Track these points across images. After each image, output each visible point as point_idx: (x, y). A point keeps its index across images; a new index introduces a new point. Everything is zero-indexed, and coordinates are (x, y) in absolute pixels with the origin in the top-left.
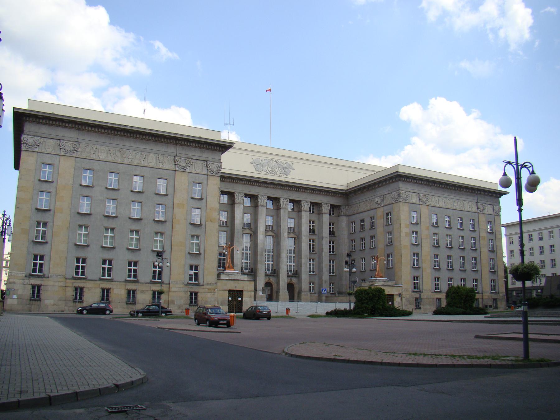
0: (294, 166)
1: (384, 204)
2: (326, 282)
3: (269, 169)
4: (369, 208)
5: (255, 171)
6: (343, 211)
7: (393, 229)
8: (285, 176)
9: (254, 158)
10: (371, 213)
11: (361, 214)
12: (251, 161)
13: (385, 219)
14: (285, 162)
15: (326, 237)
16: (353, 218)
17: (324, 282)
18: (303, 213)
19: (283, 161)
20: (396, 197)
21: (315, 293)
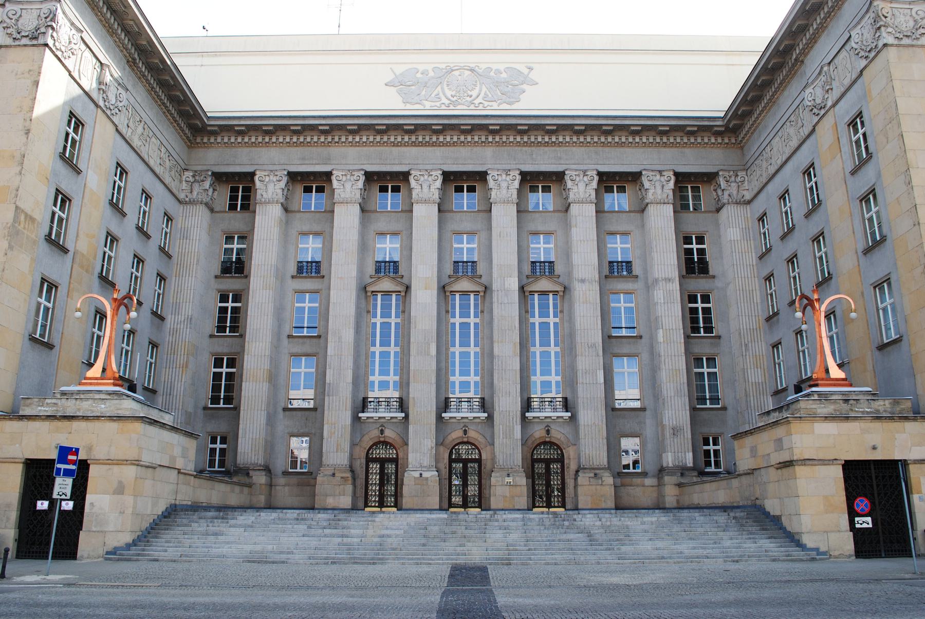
0: (533, 76)
1: (835, 94)
2: (676, 431)
3: (449, 95)
4: (794, 143)
5: (402, 106)
6: (728, 188)
7: (879, 175)
8: (508, 107)
9: (399, 69)
10: (802, 159)
11: (778, 179)
12: (390, 77)
13: (846, 148)
14: (502, 67)
15: (669, 280)
16: (759, 206)
17: (668, 433)
18: (574, 209)
19: (495, 67)
20: (868, 35)
21: (644, 474)
